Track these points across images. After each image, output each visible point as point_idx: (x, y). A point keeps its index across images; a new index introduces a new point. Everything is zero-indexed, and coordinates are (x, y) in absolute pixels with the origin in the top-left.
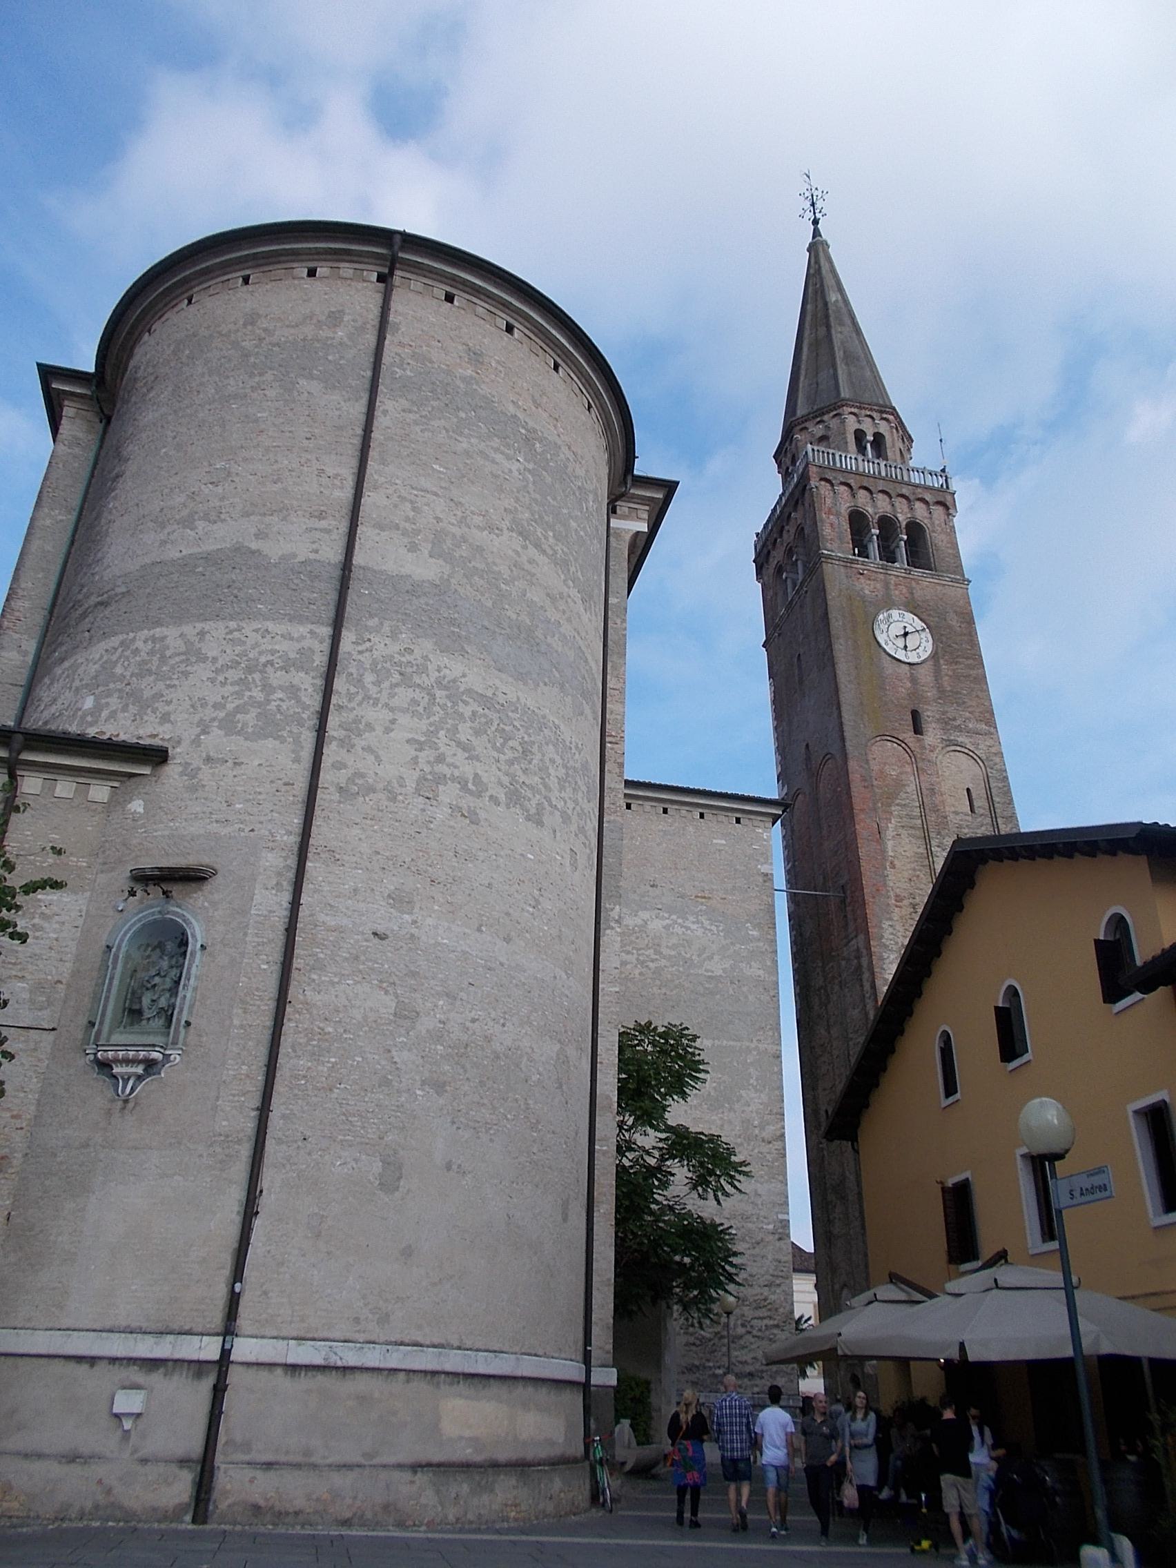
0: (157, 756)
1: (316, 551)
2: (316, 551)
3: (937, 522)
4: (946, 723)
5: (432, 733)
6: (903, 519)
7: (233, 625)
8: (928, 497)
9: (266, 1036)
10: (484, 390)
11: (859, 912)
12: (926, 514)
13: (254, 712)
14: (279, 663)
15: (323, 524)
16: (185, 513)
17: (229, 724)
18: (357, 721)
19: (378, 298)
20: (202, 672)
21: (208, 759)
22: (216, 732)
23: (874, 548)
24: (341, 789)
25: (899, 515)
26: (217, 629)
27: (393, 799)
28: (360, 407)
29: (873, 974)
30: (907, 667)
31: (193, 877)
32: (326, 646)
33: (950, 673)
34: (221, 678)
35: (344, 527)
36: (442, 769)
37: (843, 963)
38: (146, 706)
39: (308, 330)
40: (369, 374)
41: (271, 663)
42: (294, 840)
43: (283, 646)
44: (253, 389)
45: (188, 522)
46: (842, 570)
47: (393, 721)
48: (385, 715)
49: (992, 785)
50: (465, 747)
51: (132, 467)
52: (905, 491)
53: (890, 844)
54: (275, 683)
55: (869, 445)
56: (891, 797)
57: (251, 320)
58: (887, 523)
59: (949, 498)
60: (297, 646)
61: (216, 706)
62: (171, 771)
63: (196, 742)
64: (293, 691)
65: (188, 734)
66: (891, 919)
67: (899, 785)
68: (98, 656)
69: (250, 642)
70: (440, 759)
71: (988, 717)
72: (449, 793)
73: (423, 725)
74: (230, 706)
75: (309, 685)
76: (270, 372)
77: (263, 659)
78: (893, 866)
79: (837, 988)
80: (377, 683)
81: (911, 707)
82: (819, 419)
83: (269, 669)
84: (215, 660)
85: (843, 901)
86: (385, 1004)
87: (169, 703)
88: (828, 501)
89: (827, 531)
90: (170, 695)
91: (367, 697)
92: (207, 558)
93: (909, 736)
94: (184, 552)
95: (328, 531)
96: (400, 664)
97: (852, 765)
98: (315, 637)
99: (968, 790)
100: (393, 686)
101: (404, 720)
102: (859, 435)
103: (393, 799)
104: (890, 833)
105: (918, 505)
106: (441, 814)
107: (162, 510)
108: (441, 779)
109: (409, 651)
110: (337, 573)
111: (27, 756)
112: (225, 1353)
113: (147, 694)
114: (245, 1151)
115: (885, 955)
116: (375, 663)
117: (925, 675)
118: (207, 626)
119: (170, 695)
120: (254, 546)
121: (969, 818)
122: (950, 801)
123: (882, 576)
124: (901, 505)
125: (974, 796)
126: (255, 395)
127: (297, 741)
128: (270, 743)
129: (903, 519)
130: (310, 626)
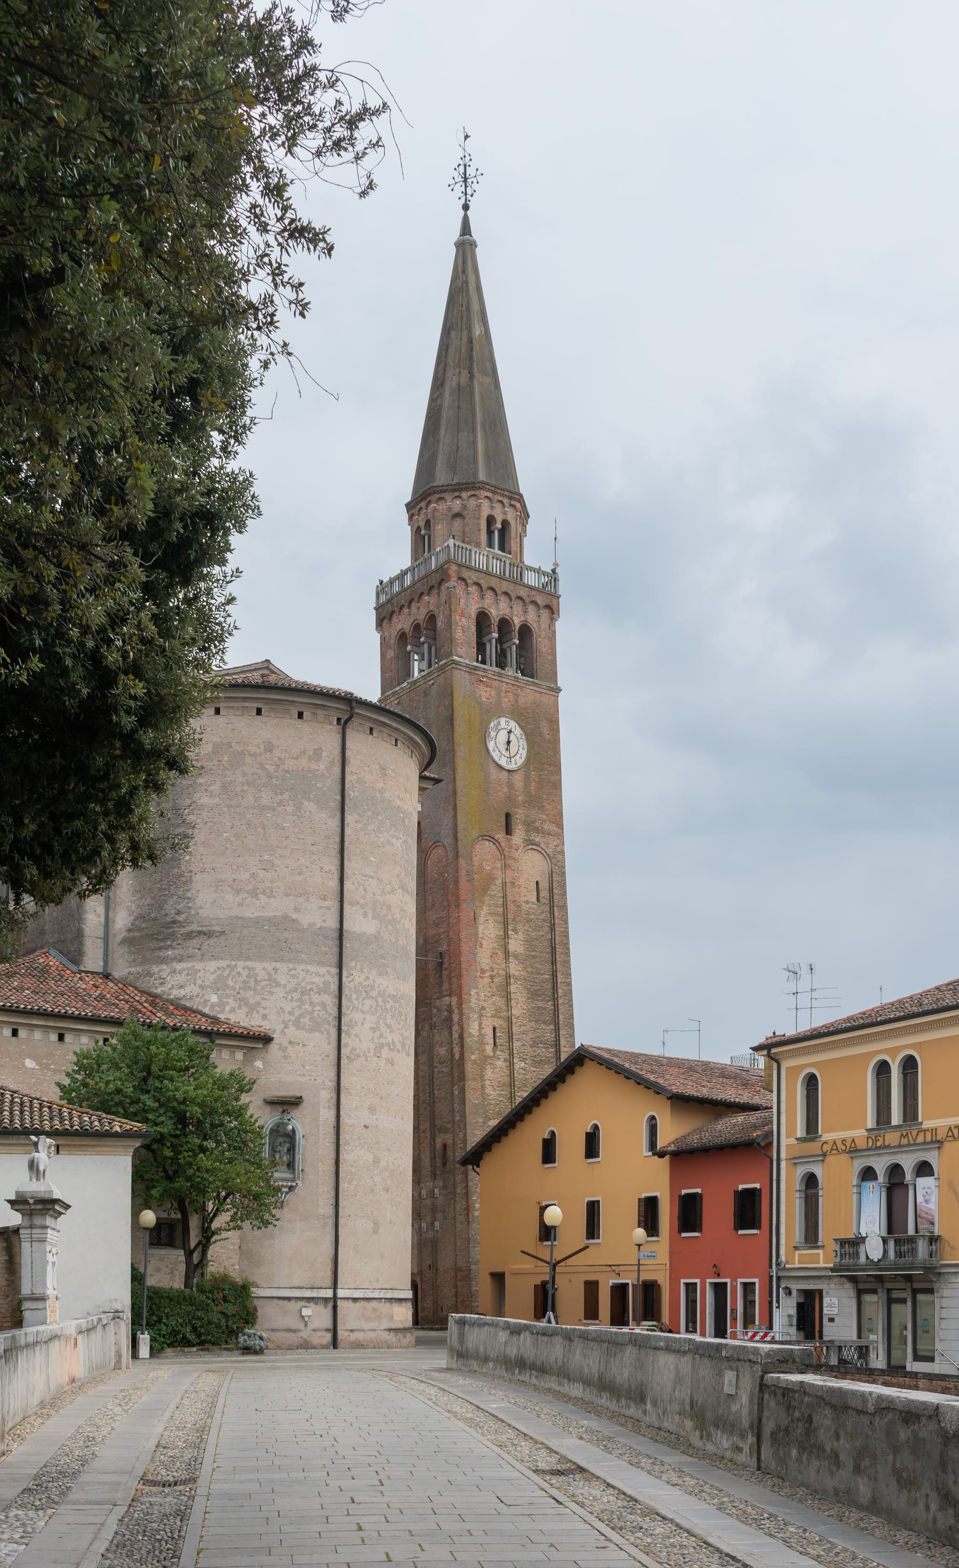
0: (266, 1040)
1: (324, 921)
2: (324, 921)
3: (543, 626)
4: (530, 826)
5: (378, 1022)
6: (517, 622)
7: (291, 966)
8: (540, 600)
9: (333, 1174)
10: (387, 795)
11: (454, 980)
12: (536, 618)
13: (308, 1017)
14: (316, 990)
15: (326, 904)
16: (250, 887)
17: (297, 1024)
18: (351, 1021)
19: (338, 737)
20: (279, 992)
21: (290, 1042)
22: (292, 1028)
23: (492, 649)
24: (348, 1058)
25: (515, 618)
26: (283, 967)
27: (367, 1060)
28: (335, 823)
29: (462, 1028)
30: (506, 774)
31: (293, 1103)
32: (336, 979)
33: (537, 779)
34: (290, 997)
35: (336, 905)
36: (383, 1041)
37: (435, 1010)
38: (252, 1009)
39: (303, 763)
40: (339, 797)
41: (311, 989)
42: (332, 1084)
43: (316, 980)
44: (279, 804)
45: (254, 893)
46: (467, 676)
47: (364, 1019)
48: (361, 1016)
49: (555, 879)
50: (389, 1026)
51: (200, 835)
52: (523, 592)
53: (481, 927)
54: (315, 1001)
55: (496, 533)
56: (485, 889)
57: (269, 748)
58: (504, 624)
59: (554, 602)
60: (323, 980)
61: (290, 1013)
62: (273, 1047)
63: (283, 1032)
64: (324, 1005)
65: (279, 1028)
66: (477, 988)
67: (491, 879)
68: (212, 970)
69: (301, 977)
70: (381, 1036)
71: (558, 820)
72: (385, 1052)
73: (374, 1018)
74: (297, 1014)
75: (330, 1001)
76: (287, 793)
77: (308, 987)
78: (481, 947)
79: (427, 1028)
80: (357, 999)
81: (506, 810)
82: (457, 494)
83: (312, 993)
84: (285, 986)
85: (441, 964)
86: (369, 1157)
87: (265, 1008)
88: (463, 601)
89: (458, 634)
90: (264, 1004)
91: (354, 1007)
92: (269, 920)
93: (501, 836)
94: (255, 915)
95: (329, 909)
96: (364, 987)
97: (462, 862)
98: (326, 974)
99: (537, 882)
100: (363, 999)
101: (368, 1017)
102: (490, 520)
103: (367, 1060)
104: (482, 919)
105: (531, 608)
106: (382, 1063)
107: (234, 880)
108: (382, 1046)
109: (368, 978)
110: (336, 935)
111: (218, 1042)
112: (335, 1294)
113: (251, 1001)
114: (331, 1221)
115: (471, 1015)
116: (355, 988)
117: (518, 780)
118: (278, 965)
119: (264, 1004)
120: (294, 916)
121: (535, 907)
122: (524, 891)
123: (496, 683)
124: (518, 608)
125: (541, 888)
126: (280, 809)
127: (328, 1033)
128: (317, 1034)
129: (517, 622)
130: (328, 968)
